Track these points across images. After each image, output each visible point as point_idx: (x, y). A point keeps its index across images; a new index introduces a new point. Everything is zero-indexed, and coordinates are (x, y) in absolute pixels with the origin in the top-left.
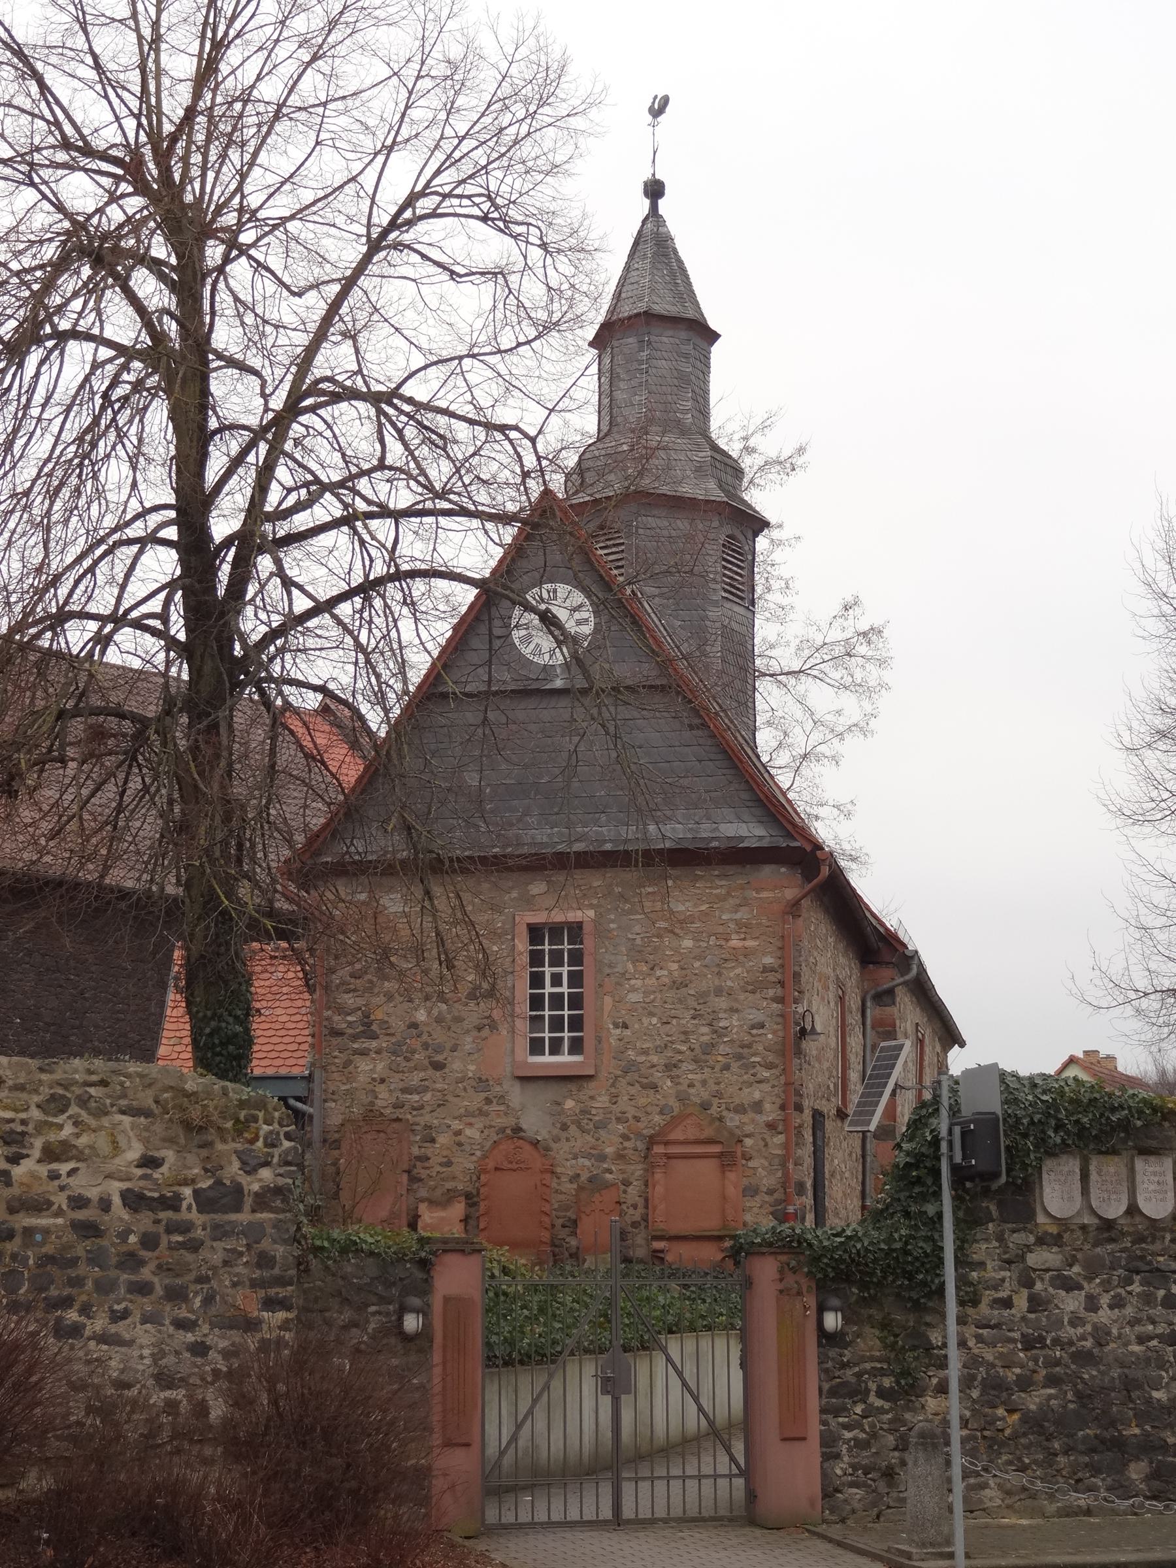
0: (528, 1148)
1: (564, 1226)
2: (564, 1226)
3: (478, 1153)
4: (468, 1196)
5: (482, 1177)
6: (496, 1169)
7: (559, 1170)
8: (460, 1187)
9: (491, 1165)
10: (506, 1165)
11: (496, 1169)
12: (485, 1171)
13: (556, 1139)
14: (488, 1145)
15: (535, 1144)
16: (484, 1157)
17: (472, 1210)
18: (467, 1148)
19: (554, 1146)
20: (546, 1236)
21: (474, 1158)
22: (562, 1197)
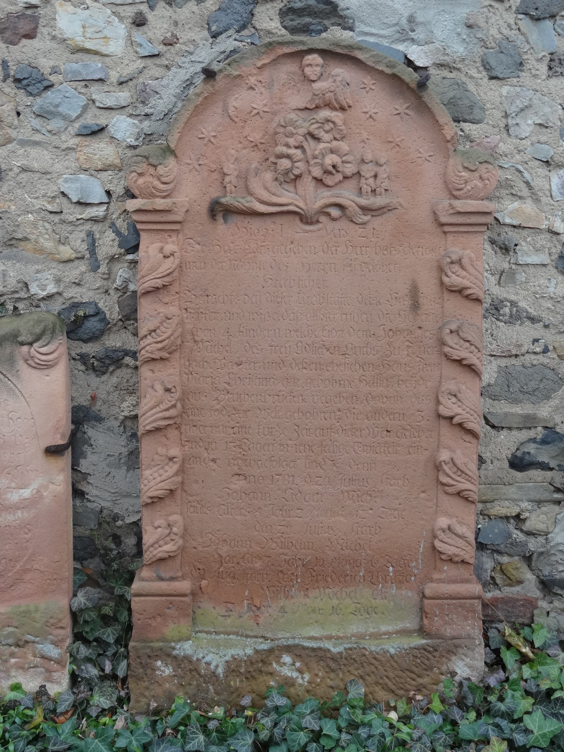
0: (374, 103)
1: (519, 463)
2: (519, 463)
3: (124, 127)
4: (77, 325)
5: (150, 248)
6: (219, 210)
7: (510, 210)
8: (43, 284)
9: (190, 192)
10: (265, 191)
11: (219, 210)
12: (165, 222)
13: (503, 64)
14: (168, 88)
15: (411, 85)
16: (155, 148)
17: (104, 385)
18: (67, 98)
19: (491, 95)
20: (457, 526)
21: (102, 151)
22: (523, 334)
